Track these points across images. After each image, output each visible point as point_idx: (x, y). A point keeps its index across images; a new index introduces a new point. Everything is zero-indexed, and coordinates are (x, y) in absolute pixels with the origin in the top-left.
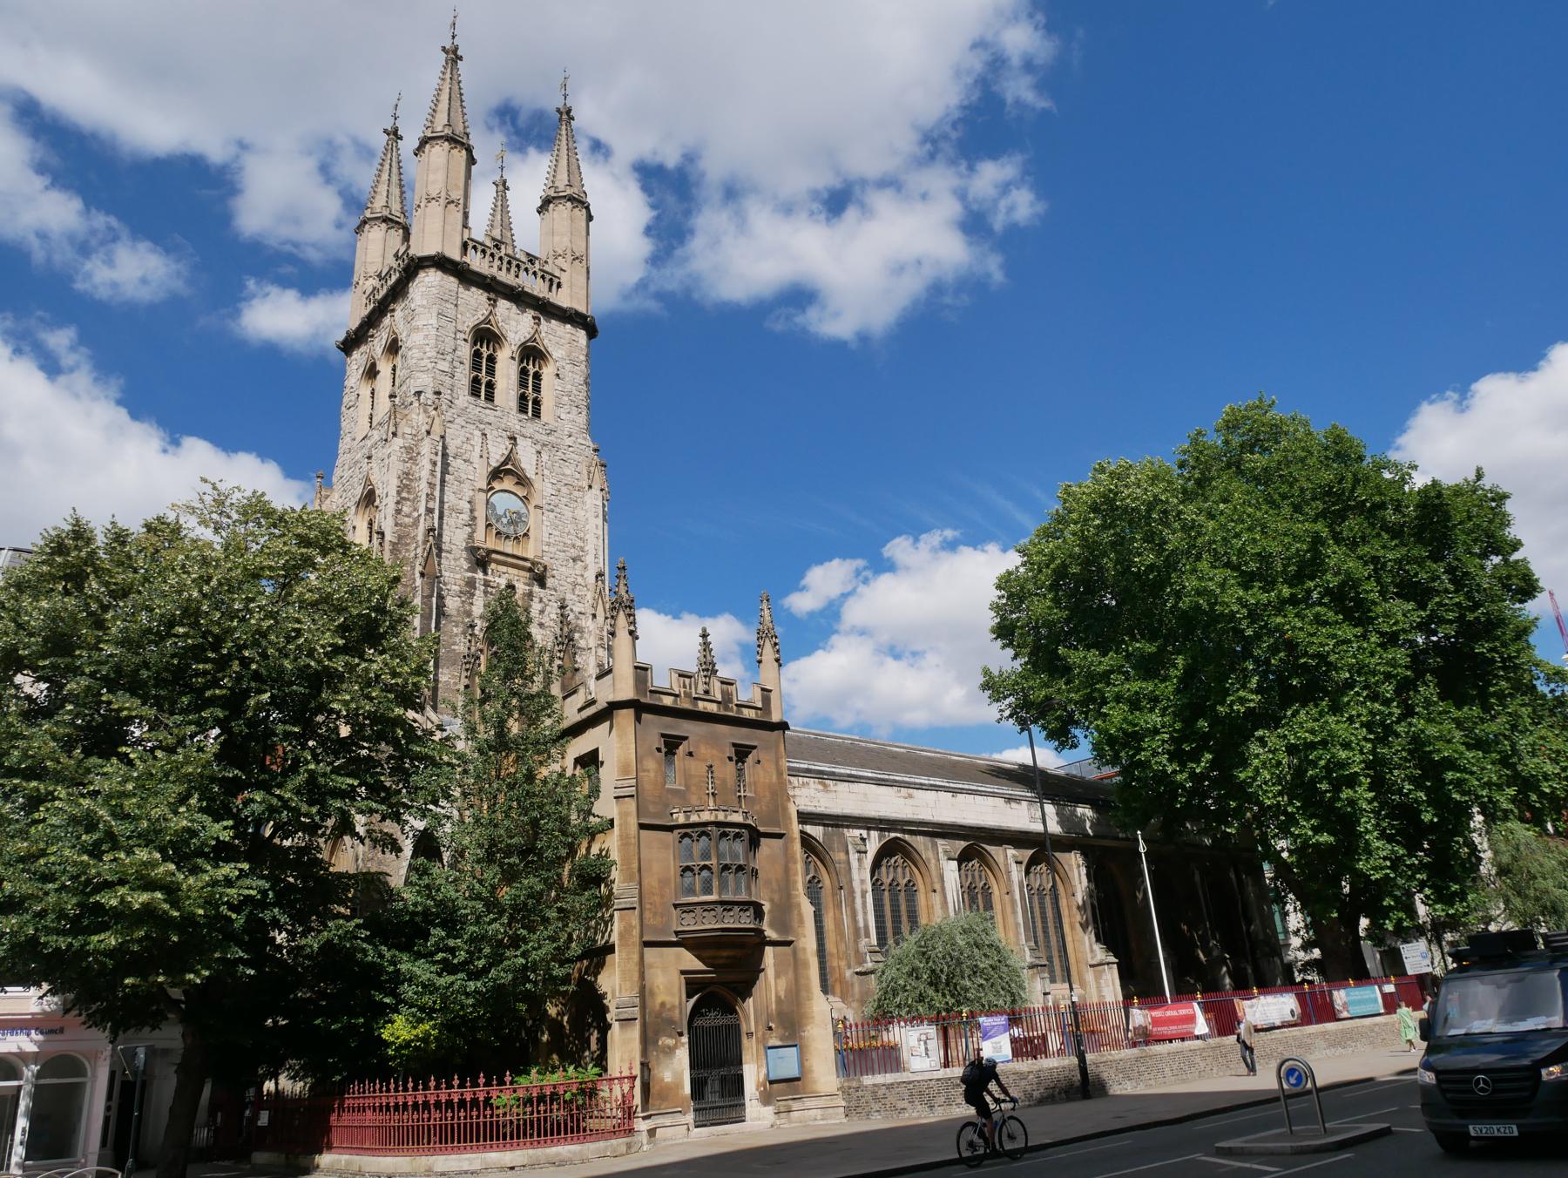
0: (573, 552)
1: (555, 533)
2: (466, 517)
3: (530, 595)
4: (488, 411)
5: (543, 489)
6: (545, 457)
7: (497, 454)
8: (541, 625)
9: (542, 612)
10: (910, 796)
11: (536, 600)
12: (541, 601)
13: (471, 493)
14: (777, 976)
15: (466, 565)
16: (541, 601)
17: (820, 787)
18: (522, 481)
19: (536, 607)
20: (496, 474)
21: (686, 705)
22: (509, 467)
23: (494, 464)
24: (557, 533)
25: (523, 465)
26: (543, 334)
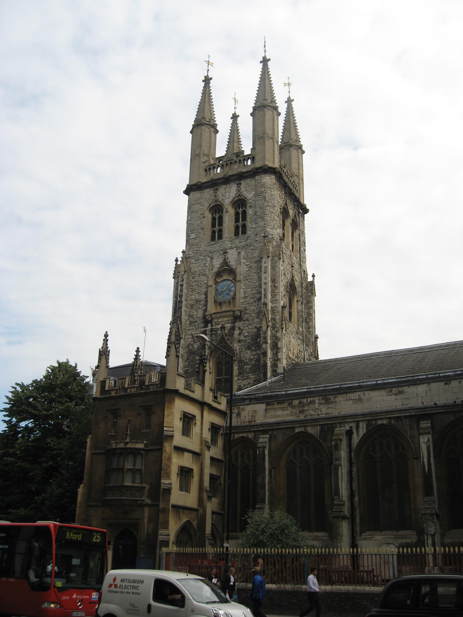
0: (258, 296)
1: (248, 290)
2: (203, 302)
3: (233, 328)
4: (215, 246)
5: (242, 270)
6: (243, 253)
7: (217, 263)
8: (239, 341)
9: (240, 334)
10: (401, 393)
11: (237, 329)
12: (239, 328)
13: (206, 289)
14: (149, 522)
15: (202, 325)
16: (239, 328)
17: (323, 401)
18: (232, 272)
19: (237, 332)
20: (218, 274)
21: (122, 393)
22: (226, 267)
23: (215, 270)
24: (250, 290)
25: (231, 263)
26: (243, 190)
